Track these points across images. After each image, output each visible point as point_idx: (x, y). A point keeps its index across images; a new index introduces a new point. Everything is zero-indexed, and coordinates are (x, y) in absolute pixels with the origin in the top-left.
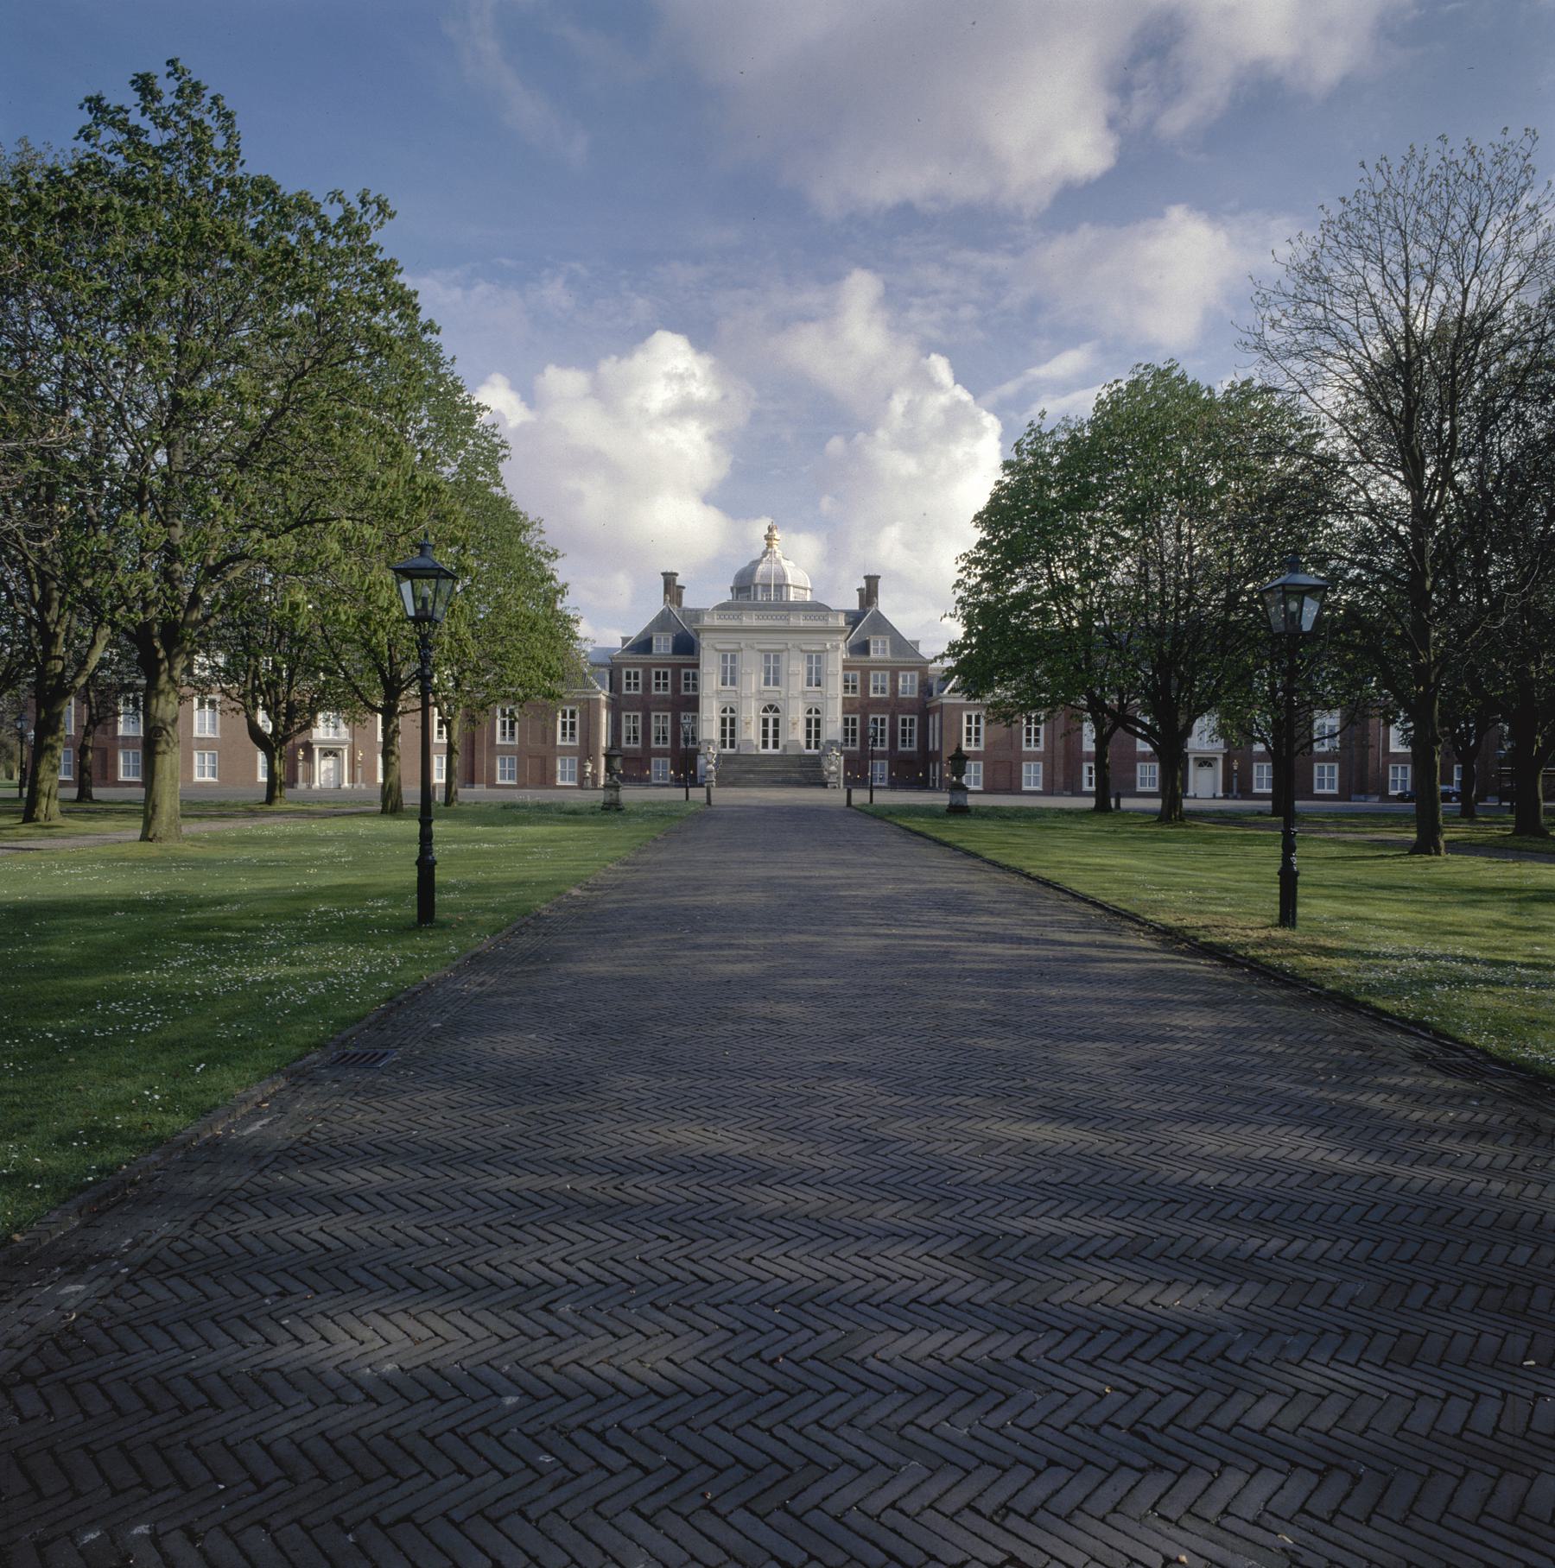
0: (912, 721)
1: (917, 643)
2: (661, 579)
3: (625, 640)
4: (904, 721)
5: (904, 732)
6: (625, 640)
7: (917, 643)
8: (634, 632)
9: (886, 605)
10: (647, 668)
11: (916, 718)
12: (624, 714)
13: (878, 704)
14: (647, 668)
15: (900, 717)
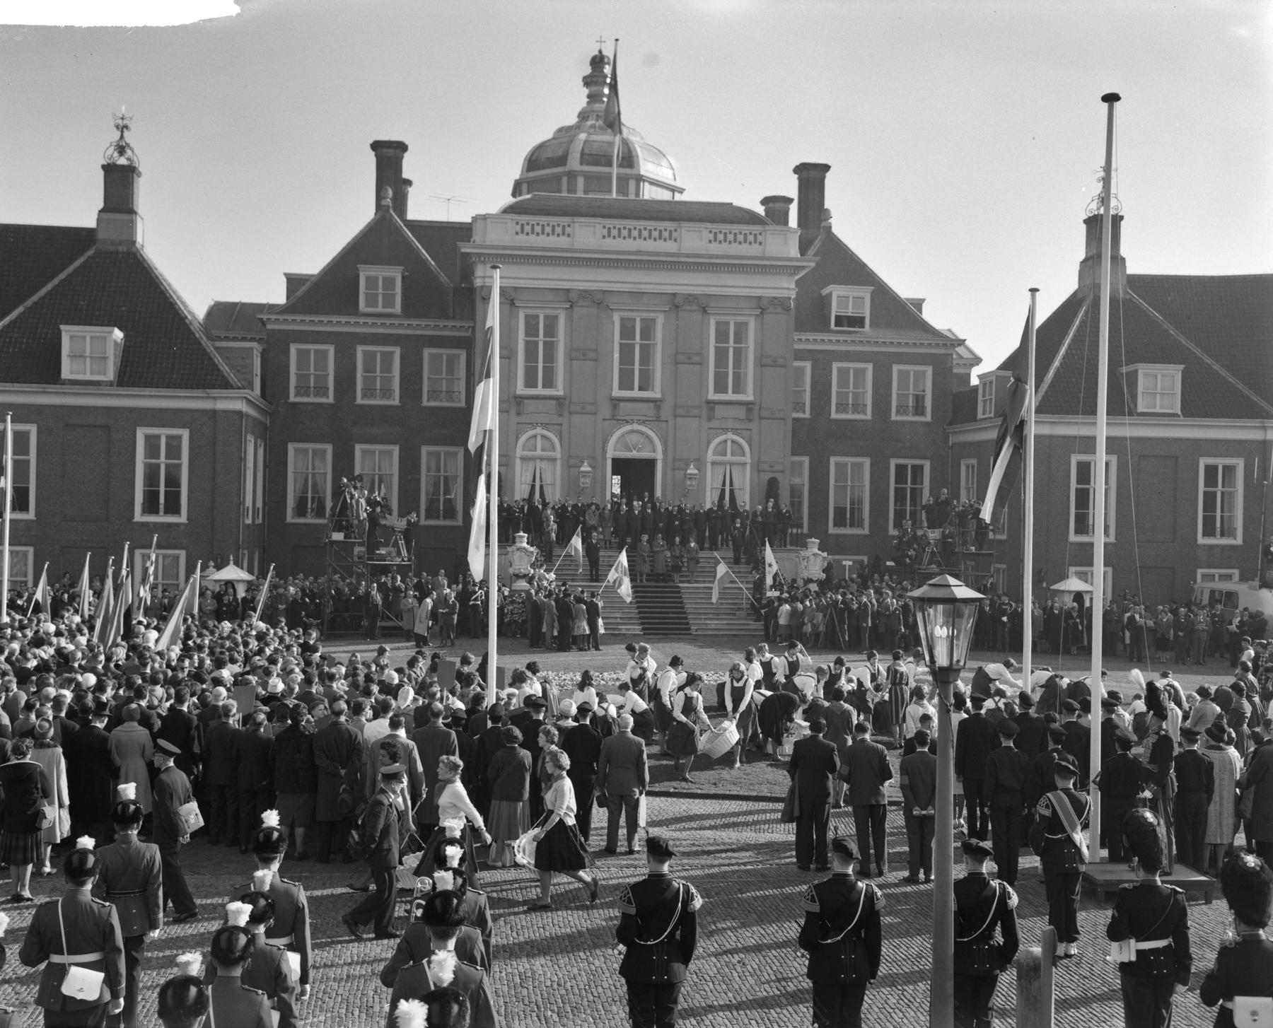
0: (918, 470)
1: (919, 304)
2: (371, 159)
3: (293, 282)
4: (901, 469)
5: (900, 495)
6: (293, 282)
7: (919, 304)
8: (313, 263)
9: (850, 222)
10: (345, 344)
11: (927, 465)
12: (291, 447)
13: (849, 437)
14: (345, 344)
15: (893, 463)
